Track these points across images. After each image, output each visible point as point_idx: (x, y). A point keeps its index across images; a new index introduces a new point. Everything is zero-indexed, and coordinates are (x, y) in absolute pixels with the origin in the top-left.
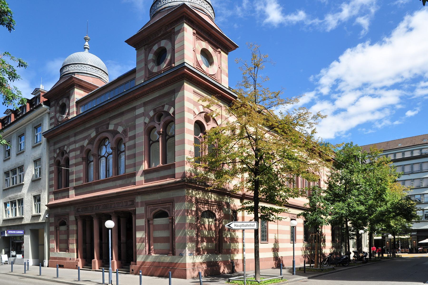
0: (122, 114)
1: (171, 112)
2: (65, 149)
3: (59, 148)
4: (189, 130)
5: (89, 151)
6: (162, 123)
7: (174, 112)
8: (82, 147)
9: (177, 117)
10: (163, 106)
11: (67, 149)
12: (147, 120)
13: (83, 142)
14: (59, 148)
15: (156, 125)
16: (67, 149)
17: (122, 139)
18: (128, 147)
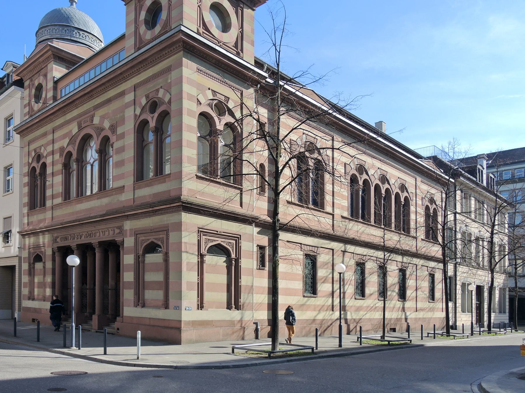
0: (109, 101)
1: (166, 100)
2: (42, 151)
3: (35, 150)
4: (188, 126)
5: (70, 154)
6: (156, 115)
7: (170, 99)
8: (62, 149)
9: (174, 107)
10: (158, 91)
11: (44, 151)
12: (138, 112)
13: (64, 140)
14: (35, 150)
15: (149, 119)
16: (44, 151)
17: (109, 138)
18: (116, 149)
